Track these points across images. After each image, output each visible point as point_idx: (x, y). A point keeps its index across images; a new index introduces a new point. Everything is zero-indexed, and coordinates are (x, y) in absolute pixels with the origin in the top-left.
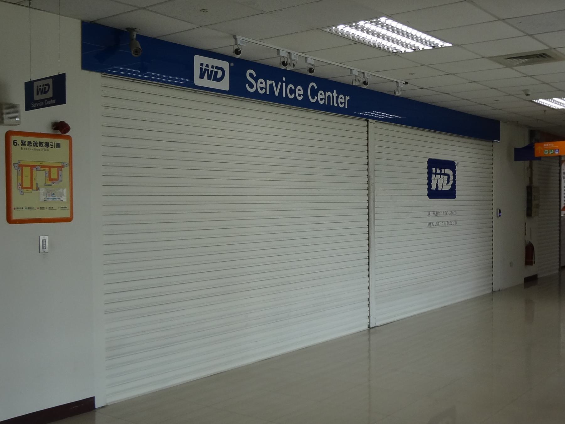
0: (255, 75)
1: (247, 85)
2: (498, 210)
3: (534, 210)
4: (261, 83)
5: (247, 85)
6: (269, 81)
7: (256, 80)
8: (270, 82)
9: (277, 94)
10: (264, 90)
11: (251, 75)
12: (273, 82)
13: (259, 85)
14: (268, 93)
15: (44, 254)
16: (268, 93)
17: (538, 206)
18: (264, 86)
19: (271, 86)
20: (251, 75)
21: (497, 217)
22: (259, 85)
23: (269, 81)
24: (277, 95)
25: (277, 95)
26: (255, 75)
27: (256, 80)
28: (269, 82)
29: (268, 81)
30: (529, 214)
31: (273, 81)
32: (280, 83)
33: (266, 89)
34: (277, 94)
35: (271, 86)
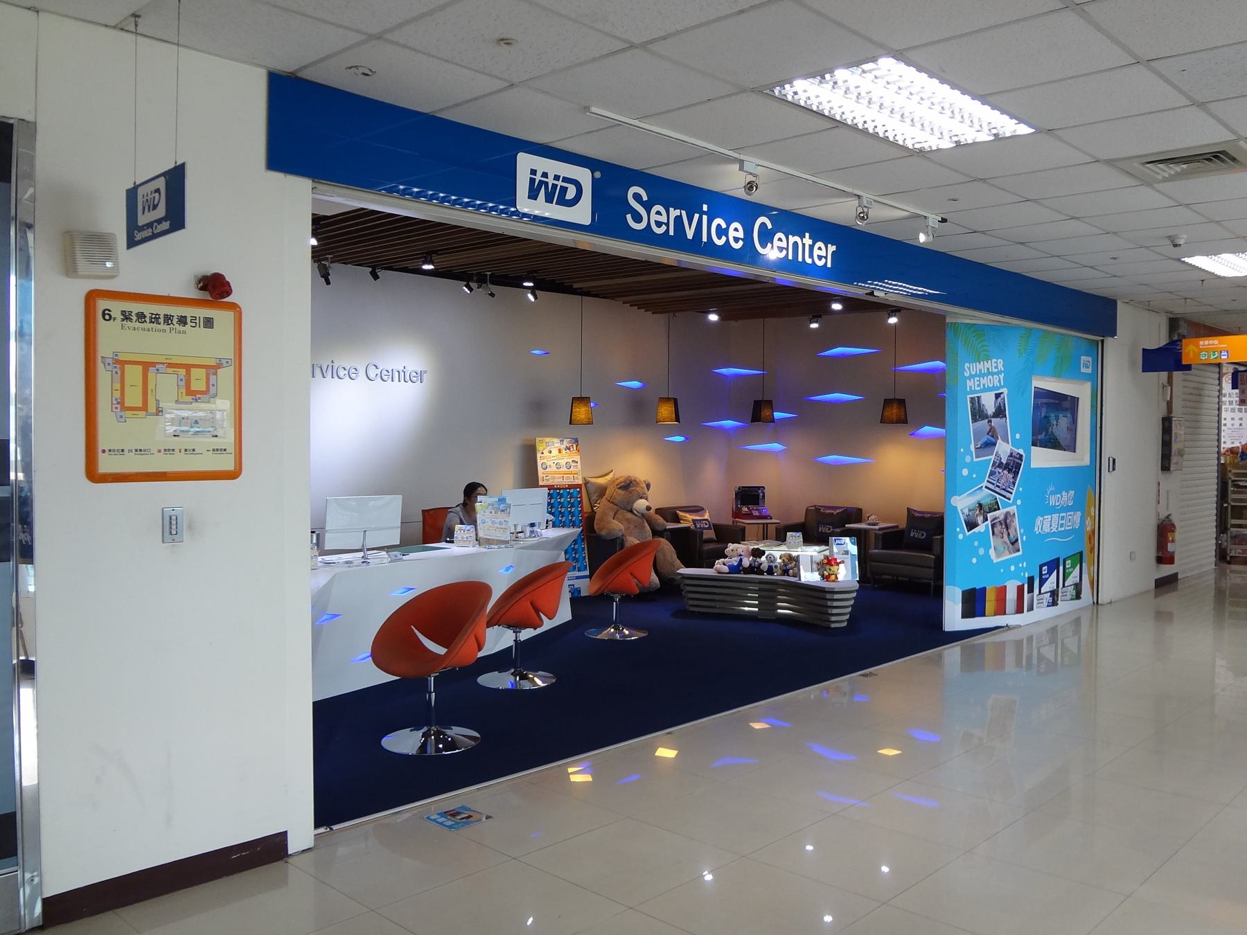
0: (645, 198)
1: (629, 217)
2: (1111, 459)
3: (1174, 459)
4: (658, 213)
5: (629, 217)
7: (648, 207)
8: (677, 212)
9: (690, 234)
10: (664, 228)
11: (637, 197)
12: (684, 213)
14: (671, 233)
15: (173, 546)
16: (671, 233)
17: (1181, 453)
18: (663, 219)
19: (678, 219)
20: (637, 197)
24: (691, 238)
25: (691, 238)
26: (645, 198)
27: (648, 207)
28: (674, 213)
29: (671, 209)
32: (697, 216)
33: (667, 224)
34: (690, 234)
35: (678, 219)
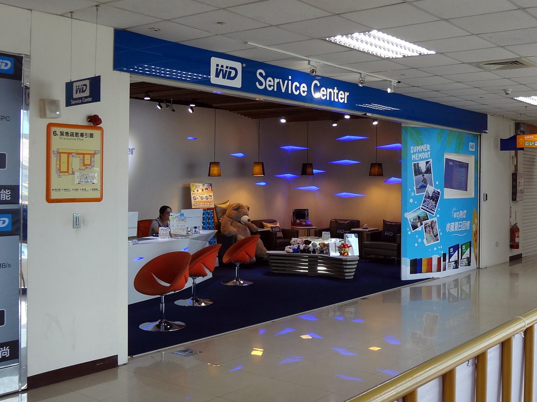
0: (264, 75)
1: (257, 83)
4: (270, 81)
5: (257, 83)
6: (277, 79)
7: (265, 78)
8: (278, 80)
9: (283, 90)
10: (272, 87)
11: (261, 74)
12: (281, 80)
13: (268, 83)
14: (275, 90)
16: (275, 90)
18: (272, 84)
19: (278, 83)
20: (261, 74)
21: (484, 201)
22: (268, 83)
23: (277, 79)
24: (284, 92)
25: (284, 92)
26: (264, 75)
27: (265, 78)
28: (277, 80)
29: (275, 79)
30: (514, 199)
31: (280, 80)
32: (286, 81)
33: (274, 86)
34: (283, 90)
35: (278, 83)
